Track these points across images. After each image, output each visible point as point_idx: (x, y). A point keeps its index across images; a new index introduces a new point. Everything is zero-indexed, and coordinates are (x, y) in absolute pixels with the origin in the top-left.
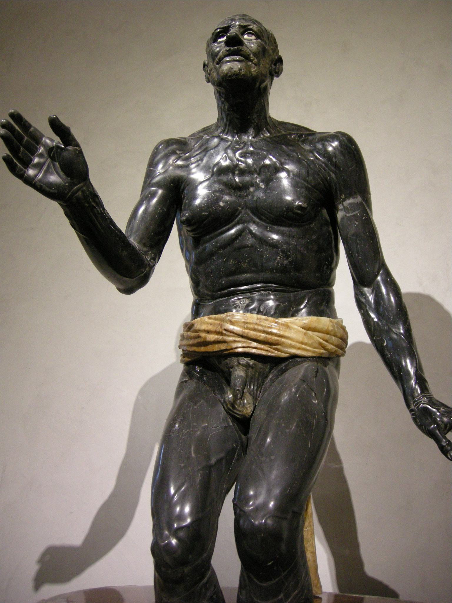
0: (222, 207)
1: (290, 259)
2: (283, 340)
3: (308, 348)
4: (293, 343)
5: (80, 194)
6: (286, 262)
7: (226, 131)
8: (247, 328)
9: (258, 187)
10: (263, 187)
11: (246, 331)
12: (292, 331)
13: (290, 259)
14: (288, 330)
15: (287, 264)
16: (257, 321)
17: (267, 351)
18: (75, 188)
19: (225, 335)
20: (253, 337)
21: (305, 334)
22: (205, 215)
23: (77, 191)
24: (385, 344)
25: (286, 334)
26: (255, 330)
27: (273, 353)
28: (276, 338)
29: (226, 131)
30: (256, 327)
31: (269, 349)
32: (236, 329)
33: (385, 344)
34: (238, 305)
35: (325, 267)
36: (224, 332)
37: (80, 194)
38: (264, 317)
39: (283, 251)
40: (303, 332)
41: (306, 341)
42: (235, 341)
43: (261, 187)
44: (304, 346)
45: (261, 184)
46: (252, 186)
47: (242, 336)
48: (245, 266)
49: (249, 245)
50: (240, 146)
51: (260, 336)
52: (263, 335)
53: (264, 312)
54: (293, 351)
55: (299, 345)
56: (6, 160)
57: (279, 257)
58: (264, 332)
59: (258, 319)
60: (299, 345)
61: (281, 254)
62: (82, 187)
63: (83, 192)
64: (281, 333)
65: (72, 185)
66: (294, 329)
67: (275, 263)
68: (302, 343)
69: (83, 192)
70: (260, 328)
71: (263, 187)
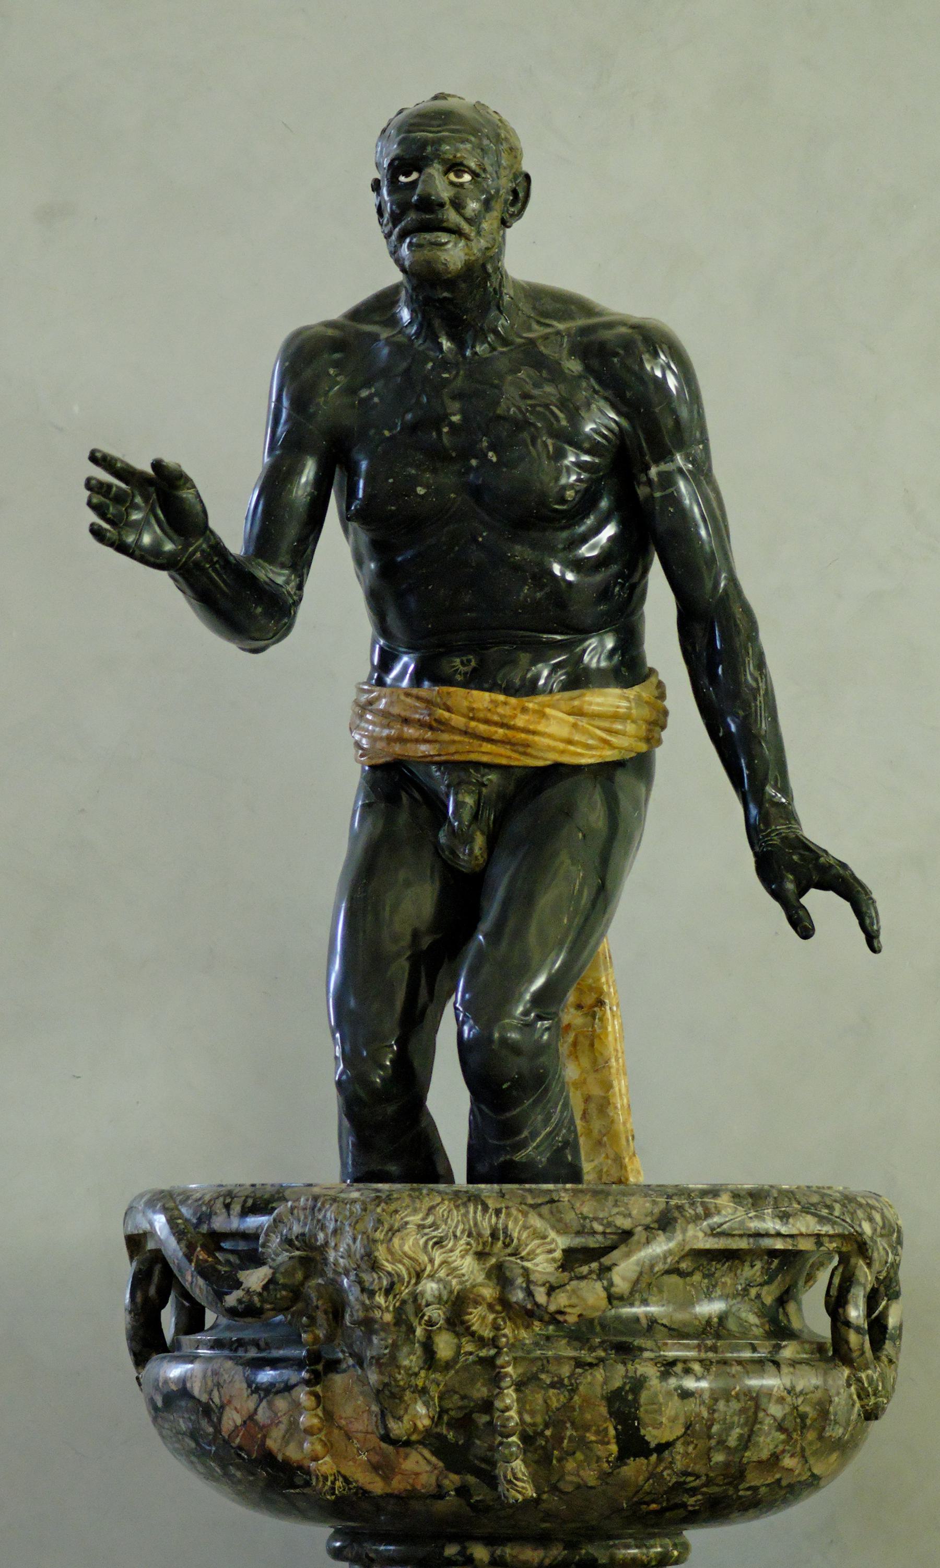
0: (422, 497)
1: (547, 589)
2: (536, 738)
3: (579, 750)
4: (552, 743)
5: (198, 554)
6: (539, 595)
7: (423, 334)
8: (473, 719)
9: (483, 457)
10: (494, 459)
11: (473, 724)
12: (552, 721)
13: (547, 589)
14: (544, 721)
15: (540, 599)
16: (490, 706)
17: (509, 757)
18: (191, 549)
19: (438, 730)
20: (485, 735)
21: (575, 726)
22: (391, 510)
23: (194, 553)
24: (721, 734)
25: (541, 728)
26: (487, 722)
27: (519, 760)
28: (523, 736)
29: (423, 334)
30: (489, 715)
31: (509, 753)
32: (458, 721)
33: (721, 734)
34: (458, 669)
35: (617, 589)
36: (434, 724)
37: (198, 554)
38: (501, 698)
39: (534, 577)
40: (568, 722)
41: (577, 737)
42: (454, 742)
43: (491, 461)
44: (572, 748)
45: (490, 454)
46: (476, 457)
47: (465, 733)
48: (467, 600)
49: (474, 564)
50: (450, 373)
51: (496, 732)
52: (501, 731)
53: (503, 686)
54: (552, 757)
55: (561, 746)
56: (97, 533)
57: (527, 587)
58: (503, 725)
59: (492, 701)
60: (561, 746)
61: (530, 581)
62: (200, 546)
63: (203, 551)
64: (531, 727)
65: (186, 546)
66: (555, 718)
67: (521, 598)
68: (570, 742)
69: (203, 551)
70: (496, 718)
71: (494, 459)
